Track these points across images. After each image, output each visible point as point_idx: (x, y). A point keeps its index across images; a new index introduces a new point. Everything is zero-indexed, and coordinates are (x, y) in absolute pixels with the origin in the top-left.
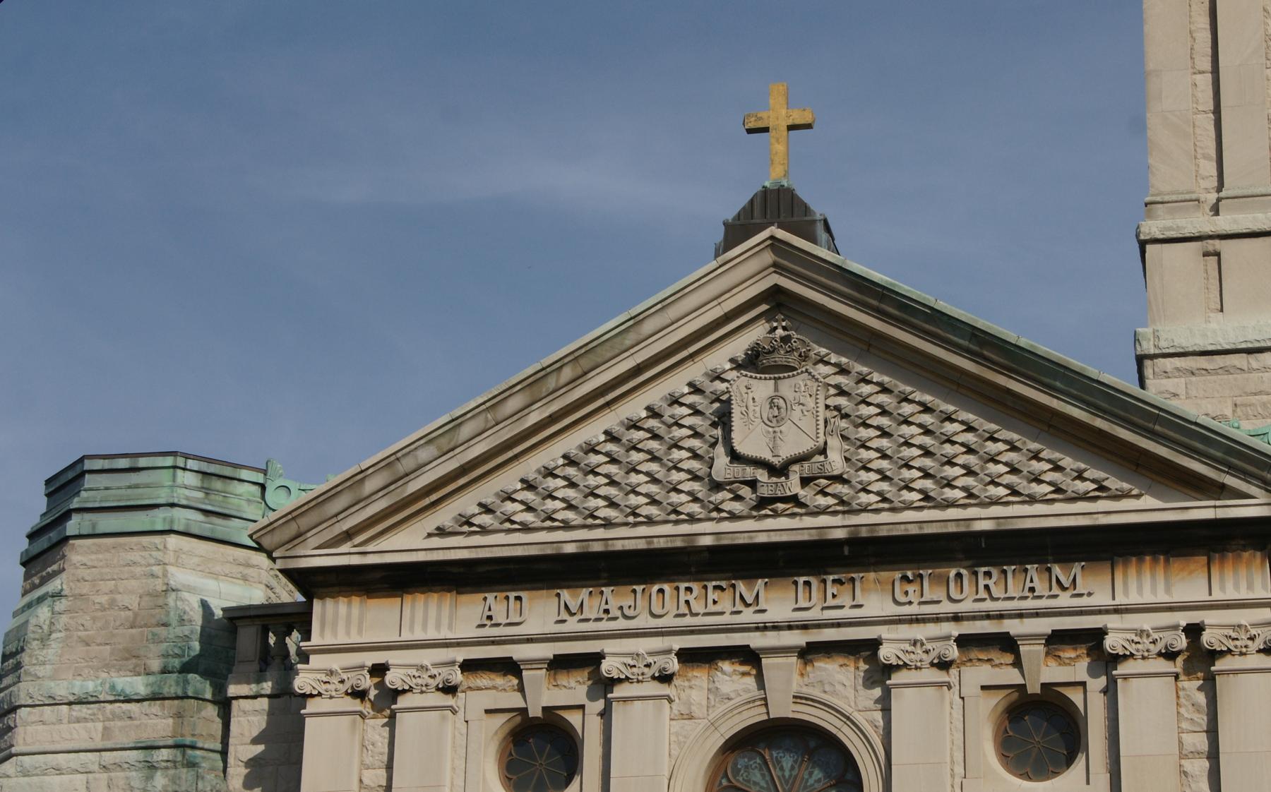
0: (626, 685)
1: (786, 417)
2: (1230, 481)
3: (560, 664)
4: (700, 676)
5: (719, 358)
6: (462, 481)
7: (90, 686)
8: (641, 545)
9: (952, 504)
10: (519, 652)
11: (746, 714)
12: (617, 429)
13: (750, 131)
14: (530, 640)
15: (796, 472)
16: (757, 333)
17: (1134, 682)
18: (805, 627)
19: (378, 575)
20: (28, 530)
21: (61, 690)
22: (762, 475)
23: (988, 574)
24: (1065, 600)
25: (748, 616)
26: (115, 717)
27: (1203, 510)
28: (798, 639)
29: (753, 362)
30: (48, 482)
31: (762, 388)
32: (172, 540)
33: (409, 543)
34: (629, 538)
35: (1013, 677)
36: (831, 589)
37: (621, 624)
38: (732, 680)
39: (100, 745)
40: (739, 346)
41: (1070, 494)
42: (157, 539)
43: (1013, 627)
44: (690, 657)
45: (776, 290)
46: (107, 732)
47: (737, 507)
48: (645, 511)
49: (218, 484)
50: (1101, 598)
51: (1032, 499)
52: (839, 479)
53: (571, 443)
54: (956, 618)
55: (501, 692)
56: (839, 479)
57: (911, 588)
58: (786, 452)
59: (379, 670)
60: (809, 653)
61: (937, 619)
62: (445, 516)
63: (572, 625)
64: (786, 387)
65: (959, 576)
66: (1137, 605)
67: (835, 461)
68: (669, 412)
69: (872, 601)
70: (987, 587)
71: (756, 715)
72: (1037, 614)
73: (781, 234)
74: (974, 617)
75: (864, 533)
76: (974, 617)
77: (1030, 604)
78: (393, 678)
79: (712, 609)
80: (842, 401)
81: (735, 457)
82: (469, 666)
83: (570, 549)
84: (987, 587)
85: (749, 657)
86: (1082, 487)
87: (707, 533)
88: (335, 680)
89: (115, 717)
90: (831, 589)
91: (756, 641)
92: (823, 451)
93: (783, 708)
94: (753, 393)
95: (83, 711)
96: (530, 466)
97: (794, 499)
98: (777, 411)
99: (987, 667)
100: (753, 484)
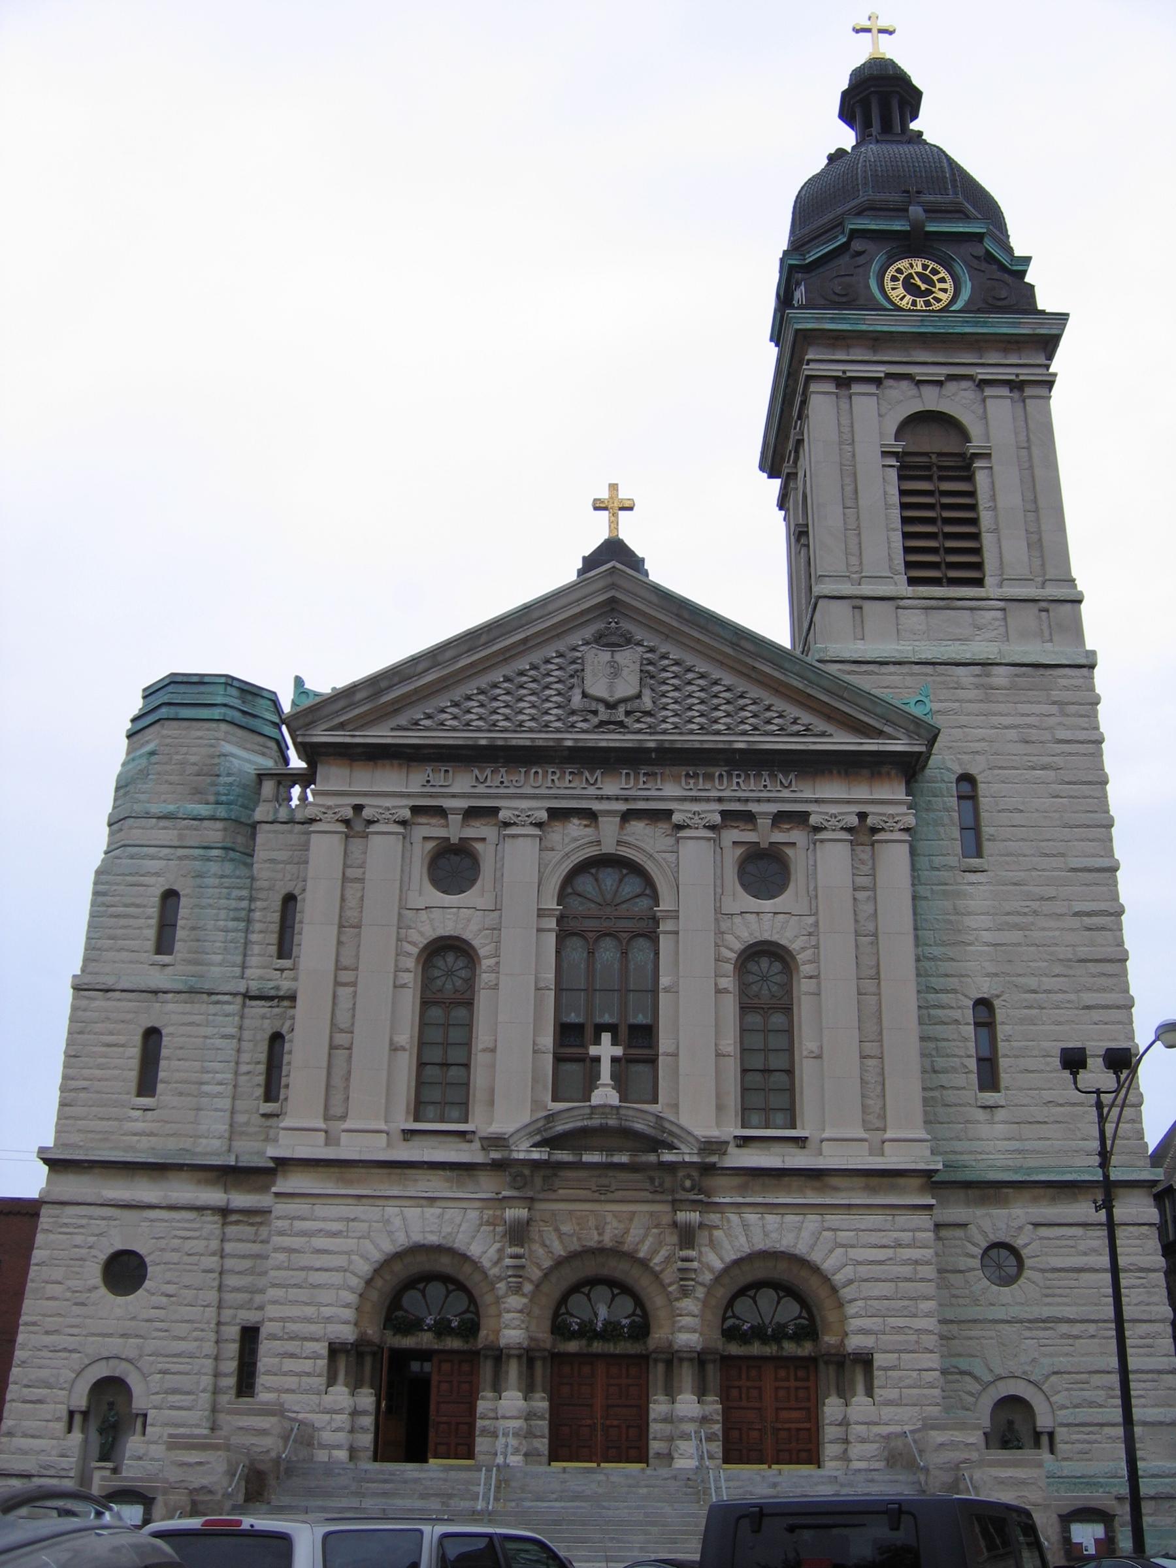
0: (514, 827)
1: (611, 676)
2: (886, 729)
3: (472, 814)
4: (558, 827)
5: (575, 639)
6: (414, 698)
7: (171, 808)
8: (528, 743)
9: (718, 733)
10: (447, 803)
11: (587, 850)
12: (511, 674)
13: (596, 509)
14: (454, 796)
15: (622, 709)
16: (600, 625)
17: (828, 845)
18: (626, 800)
19: (359, 750)
20: (131, 717)
21: (155, 809)
22: (601, 708)
23: (738, 776)
24: (786, 794)
25: (592, 791)
26: (187, 828)
27: (871, 745)
28: (622, 807)
29: (600, 640)
30: (144, 690)
31: (605, 656)
32: (224, 727)
33: (381, 734)
34: (521, 739)
35: (751, 837)
36: (642, 779)
37: (512, 791)
38: (575, 829)
39: (177, 843)
40: (588, 632)
41: (788, 731)
42: (214, 725)
43: (754, 807)
44: (556, 814)
45: (613, 600)
46: (181, 837)
47: (584, 725)
48: (528, 724)
49: (250, 697)
50: (808, 795)
51: (767, 734)
52: (648, 713)
53: (483, 681)
54: (720, 800)
55: (433, 829)
56: (648, 713)
57: (692, 781)
58: (620, 693)
59: (358, 808)
60: (627, 816)
61: (708, 800)
62: (402, 720)
63: (481, 789)
64: (619, 657)
65: (721, 776)
66: (831, 798)
67: (647, 702)
68: (544, 668)
69: (668, 790)
70: (738, 783)
71: (592, 851)
72: (769, 800)
73: (619, 566)
74: (731, 800)
75: (667, 745)
76: (731, 800)
77: (765, 794)
78: (367, 813)
79: (571, 788)
80: (650, 668)
81: (585, 695)
82: (415, 810)
83: (483, 742)
84: (738, 783)
85: (590, 816)
86: (796, 728)
87: (569, 740)
88: (330, 812)
89: (187, 828)
90: (642, 779)
91: (596, 806)
92: (639, 696)
93: (609, 847)
94: (597, 659)
95: (163, 823)
96: (457, 694)
97: (621, 724)
98: (615, 671)
99: (736, 831)
100: (595, 713)
